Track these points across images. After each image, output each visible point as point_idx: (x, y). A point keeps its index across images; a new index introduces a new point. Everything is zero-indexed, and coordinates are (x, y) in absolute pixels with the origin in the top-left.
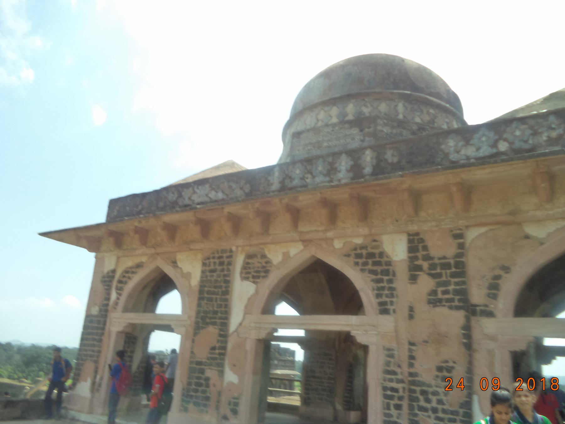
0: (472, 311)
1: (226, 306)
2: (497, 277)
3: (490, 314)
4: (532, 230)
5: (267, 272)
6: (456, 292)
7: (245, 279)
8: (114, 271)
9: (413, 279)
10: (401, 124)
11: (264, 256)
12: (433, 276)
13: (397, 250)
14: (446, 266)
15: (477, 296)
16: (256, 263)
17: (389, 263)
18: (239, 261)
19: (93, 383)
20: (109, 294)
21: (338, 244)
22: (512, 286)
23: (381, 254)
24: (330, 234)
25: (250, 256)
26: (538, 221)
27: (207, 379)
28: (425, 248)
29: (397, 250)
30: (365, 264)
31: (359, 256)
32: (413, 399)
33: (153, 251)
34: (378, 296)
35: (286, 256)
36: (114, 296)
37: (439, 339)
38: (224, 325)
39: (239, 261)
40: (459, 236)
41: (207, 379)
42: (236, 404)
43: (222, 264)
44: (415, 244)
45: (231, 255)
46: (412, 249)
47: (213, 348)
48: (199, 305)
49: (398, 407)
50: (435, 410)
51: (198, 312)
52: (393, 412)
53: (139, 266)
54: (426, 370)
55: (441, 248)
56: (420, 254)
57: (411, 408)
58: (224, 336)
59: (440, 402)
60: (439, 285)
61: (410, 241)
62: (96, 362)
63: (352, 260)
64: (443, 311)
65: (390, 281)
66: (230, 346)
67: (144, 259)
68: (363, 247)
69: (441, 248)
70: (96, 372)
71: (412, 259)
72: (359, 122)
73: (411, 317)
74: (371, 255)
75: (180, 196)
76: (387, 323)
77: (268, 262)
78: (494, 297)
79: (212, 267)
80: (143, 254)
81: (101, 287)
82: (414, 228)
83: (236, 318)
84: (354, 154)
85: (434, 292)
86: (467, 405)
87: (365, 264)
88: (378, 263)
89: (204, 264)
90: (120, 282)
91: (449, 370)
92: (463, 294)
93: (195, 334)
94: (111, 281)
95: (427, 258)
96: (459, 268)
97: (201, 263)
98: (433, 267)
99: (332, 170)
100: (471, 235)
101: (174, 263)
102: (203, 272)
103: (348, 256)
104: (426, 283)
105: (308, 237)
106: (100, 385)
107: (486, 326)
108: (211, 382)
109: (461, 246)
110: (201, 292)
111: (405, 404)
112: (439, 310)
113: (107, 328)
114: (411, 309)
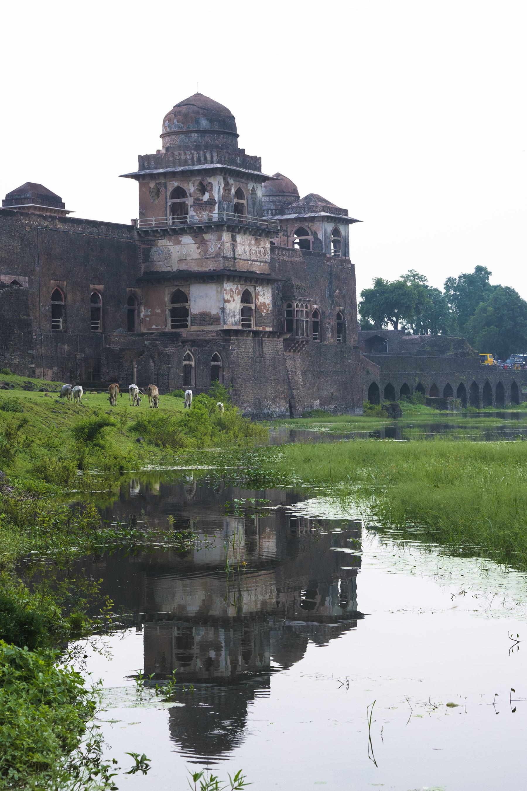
10: (280, 202)
15: (289, 234)
72: (273, 202)
84: (272, 210)
92: (287, 234)
96: (287, 231)
99: (268, 213)
107: (290, 238)
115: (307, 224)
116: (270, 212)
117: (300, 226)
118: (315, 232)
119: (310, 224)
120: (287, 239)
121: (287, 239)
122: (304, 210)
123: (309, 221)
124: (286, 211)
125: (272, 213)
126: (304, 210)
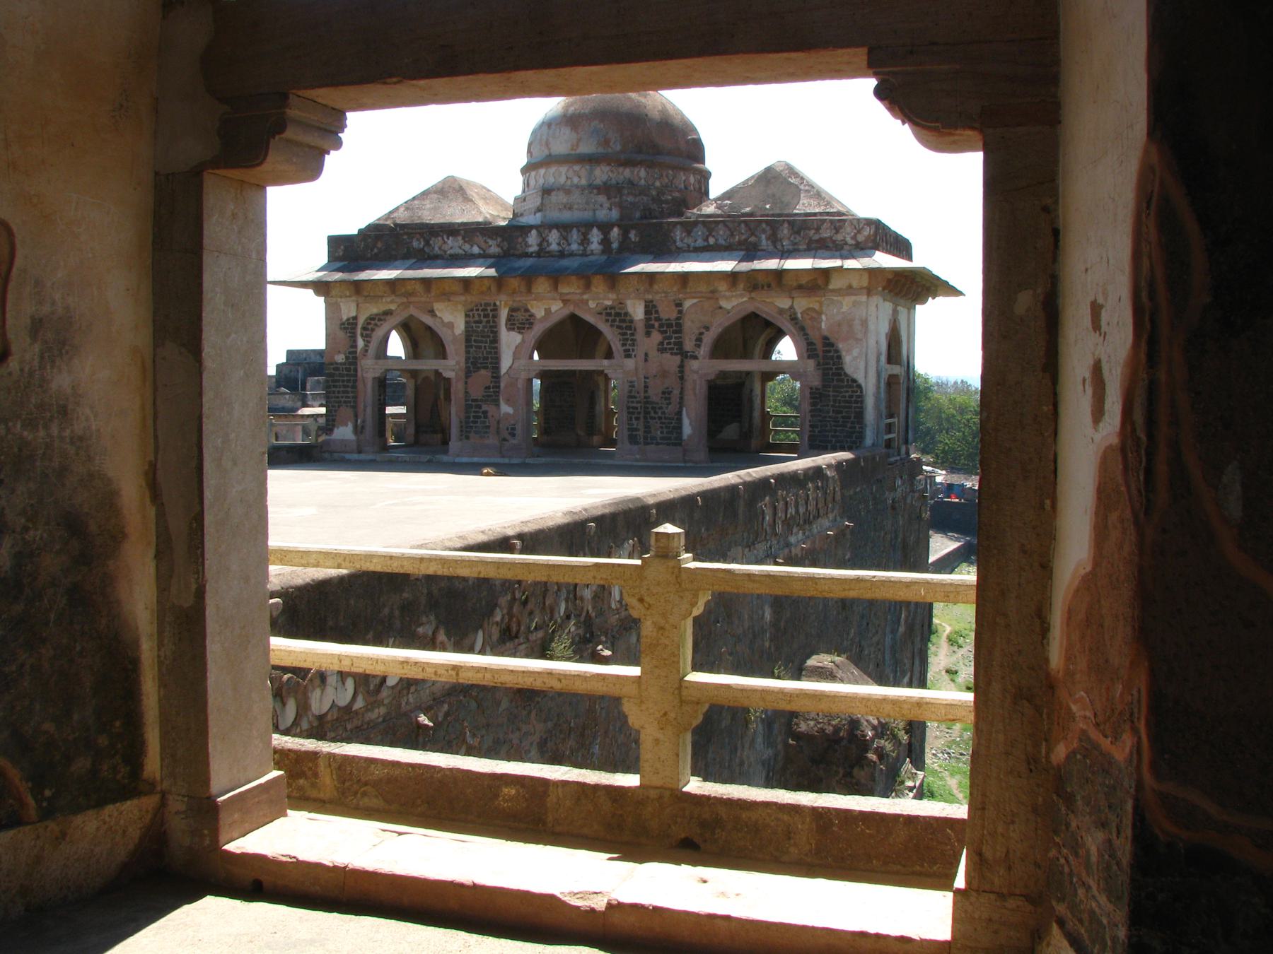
0: (685, 355)
1: (496, 353)
2: (701, 334)
3: (696, 358)
4: (724, 303)
5: (532, 324)
6: (675, 344)
7: (510, 329)
8: (355, 318)
9: (648, 334)
10: (644, 191)
11: (527, 310)
12: (662, 332)
13: (637, 311)
14: (669, 326)
15: (689, 345)
16: (520, 316)
17: (631, 321)
18: (504, 314)
19: (355, 427)
20: (355, 341)
21: (592, 304)
22: (708, 339)
23: (626, 314)
24: (585, 297)
25: (512, 310)
26: (727, 298)
27: (485, 413)
28: (657, 312)
29: (637, 311)
30: (614, 321)
31: (609, 315)
32: (647, 413)
33: (405, 300)
34: (623, 345)
35: (548, 311)
36: (360, 343)
37: (664, 374)
38: (496, 368)
39: (504, 314)
40: (679, 305)
41: (485, 413)
42: (514, 429)
43: (486, 316)
44: (650, 308)
45: (495, 309)
46: (647, 312)
47: (488, 388)
48: (468, 352)
49: (637, 419)
50: (660, 418)
51: (467, 359)
52: (634, 421)
53: (388, 313)
54: (655, 394)
55: (667, 312)
56: (653, 316)
57: (645, 418)
58: (496, 377)
59: (663, 413)
60: (665, 338)
61: (646, 306)
62: (355, 407)
63: (604, 317)
64: (667, 355)
65: (632, 334)
66: (502, 385)
67: (393, 307)
68: (612, 308)
69: (667, 312)
70: (356, 416)
71: (647, 319)
72: (606, 189)
73: (646, 360)
74: (618, 314)
75: (427, 243)
76: (630, 364)
77: (532, 315)
78: (699, 346)
79: (477, 318)
80: (392, 302)
81: (341, 335)
82: (650, 297)
83: (506, 363)
84: (605, 228)
85: (662, 343)
86: (679, 413)
87: (614, 321)
88: (624, 321)
89: (467, 316)
90: (364, 329)
91: (670, 393)
92: (680, 344)
93: (467, 377)
94: (355, 328)
95: (658, 319)
97: (463, 315)
98: (661, 326)
99: (585, 241)
100: (687, 304)
101: (432, 312)
102: (467, 322)
103: (600, 314)
104: (656, 337)
105: (568, 297)
106: (363, 427)
107: (694, 365)
108: (490, 414)
109: (680, 312)
110: (468, 340)
111: (642, 416)
112: (664, 355)
113: (359, 374)
114: (646, 355)
115: (784, 303)
116: (595, 236)
117: (751, 308)
118: (828, 343)
119: (802, 304)
120: (681, 366)
121: (681, 366)
122: (774, 238)
123: (800, 287)
124: (678, 234)
125: (606, 242)
126: (774, 238)
